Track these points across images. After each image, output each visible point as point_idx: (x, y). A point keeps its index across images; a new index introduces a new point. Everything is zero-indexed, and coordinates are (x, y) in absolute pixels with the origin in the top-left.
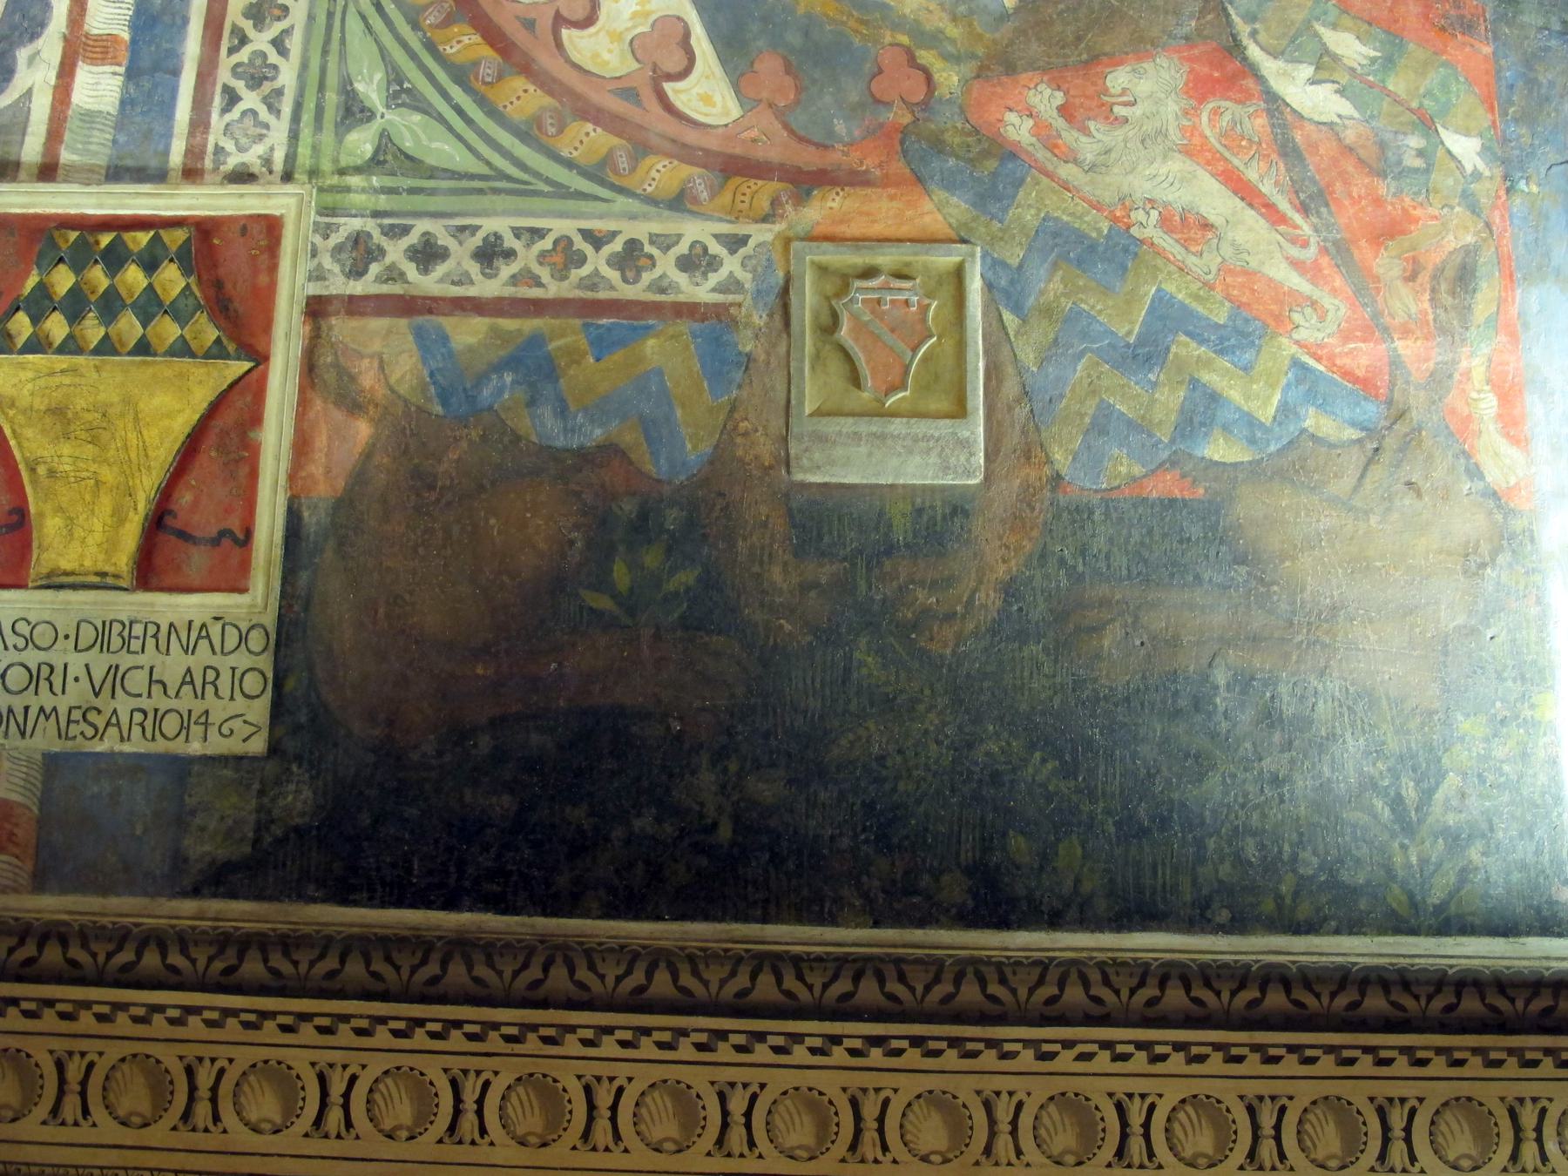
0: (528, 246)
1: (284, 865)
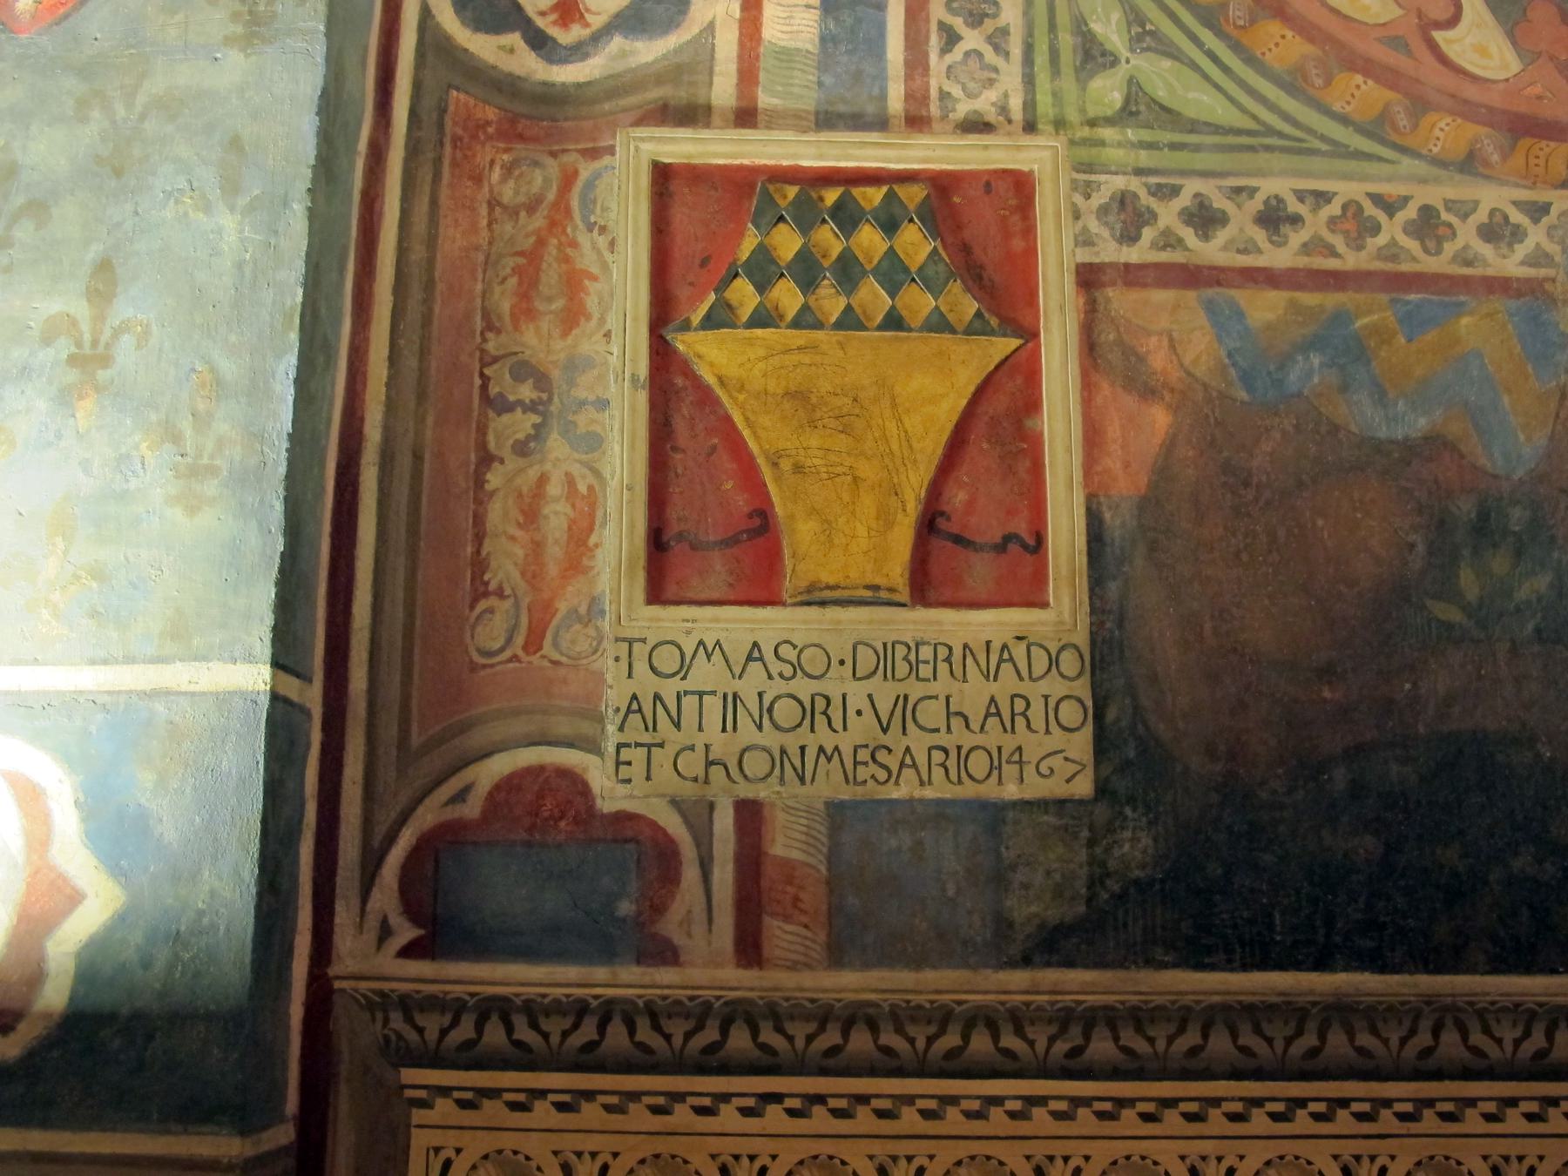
0: (1315, 209)
1: (1125, 925)
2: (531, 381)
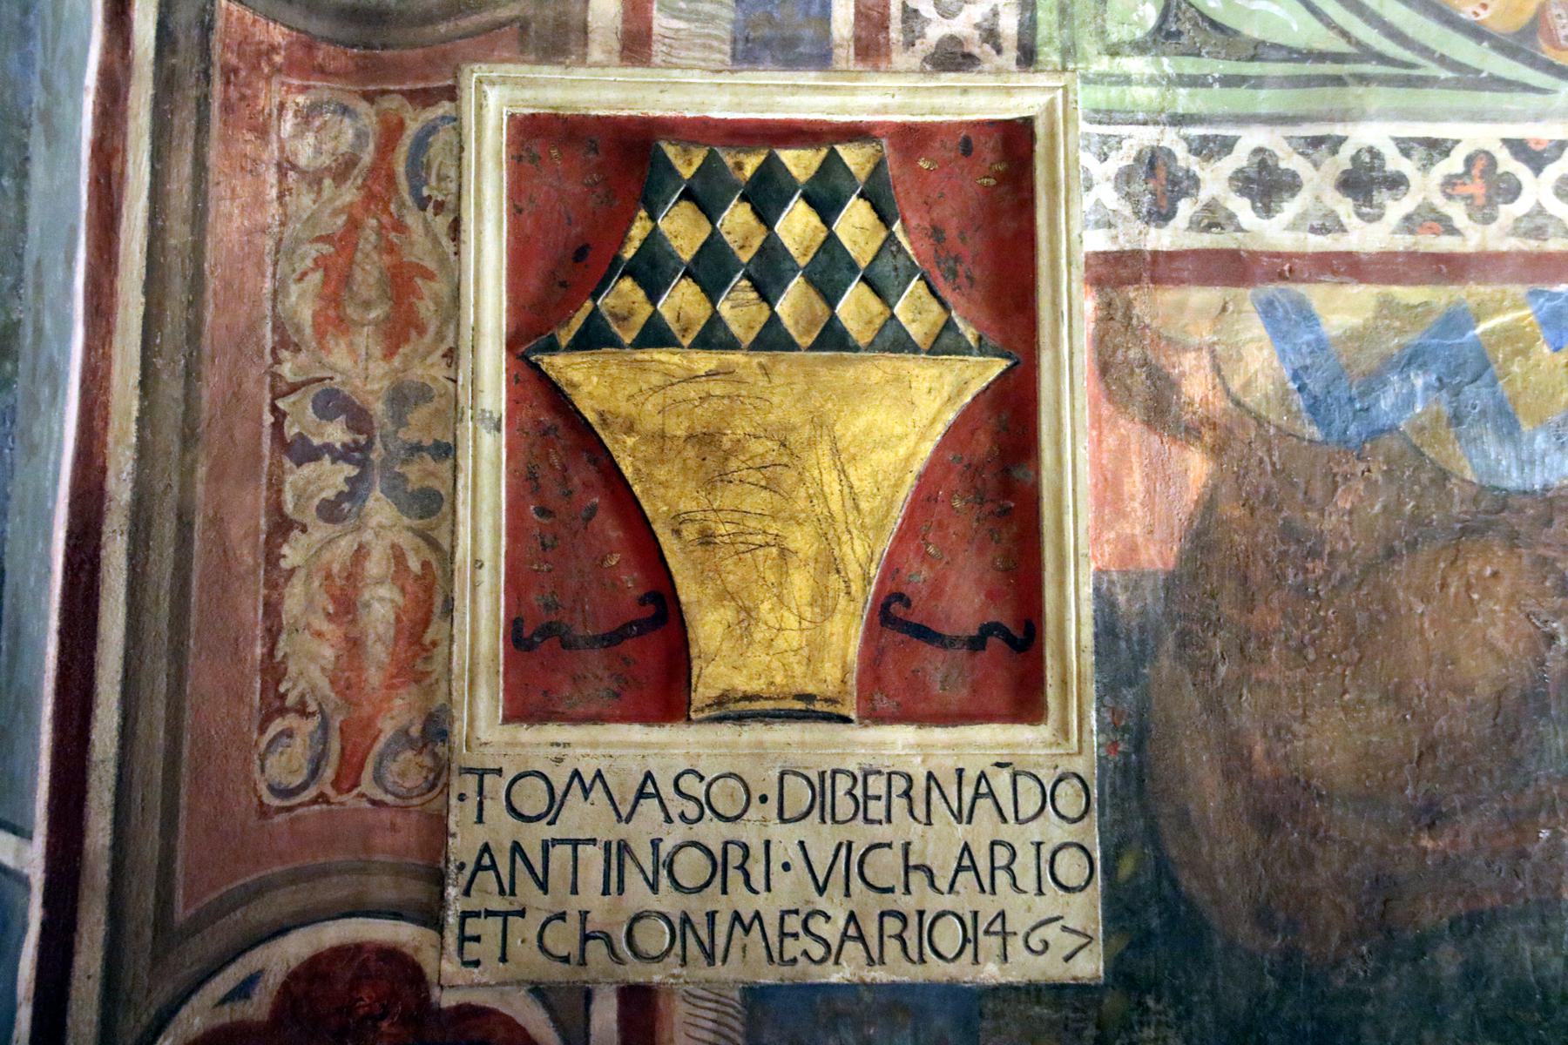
0: (1425, 167)
2: (342, 418)
